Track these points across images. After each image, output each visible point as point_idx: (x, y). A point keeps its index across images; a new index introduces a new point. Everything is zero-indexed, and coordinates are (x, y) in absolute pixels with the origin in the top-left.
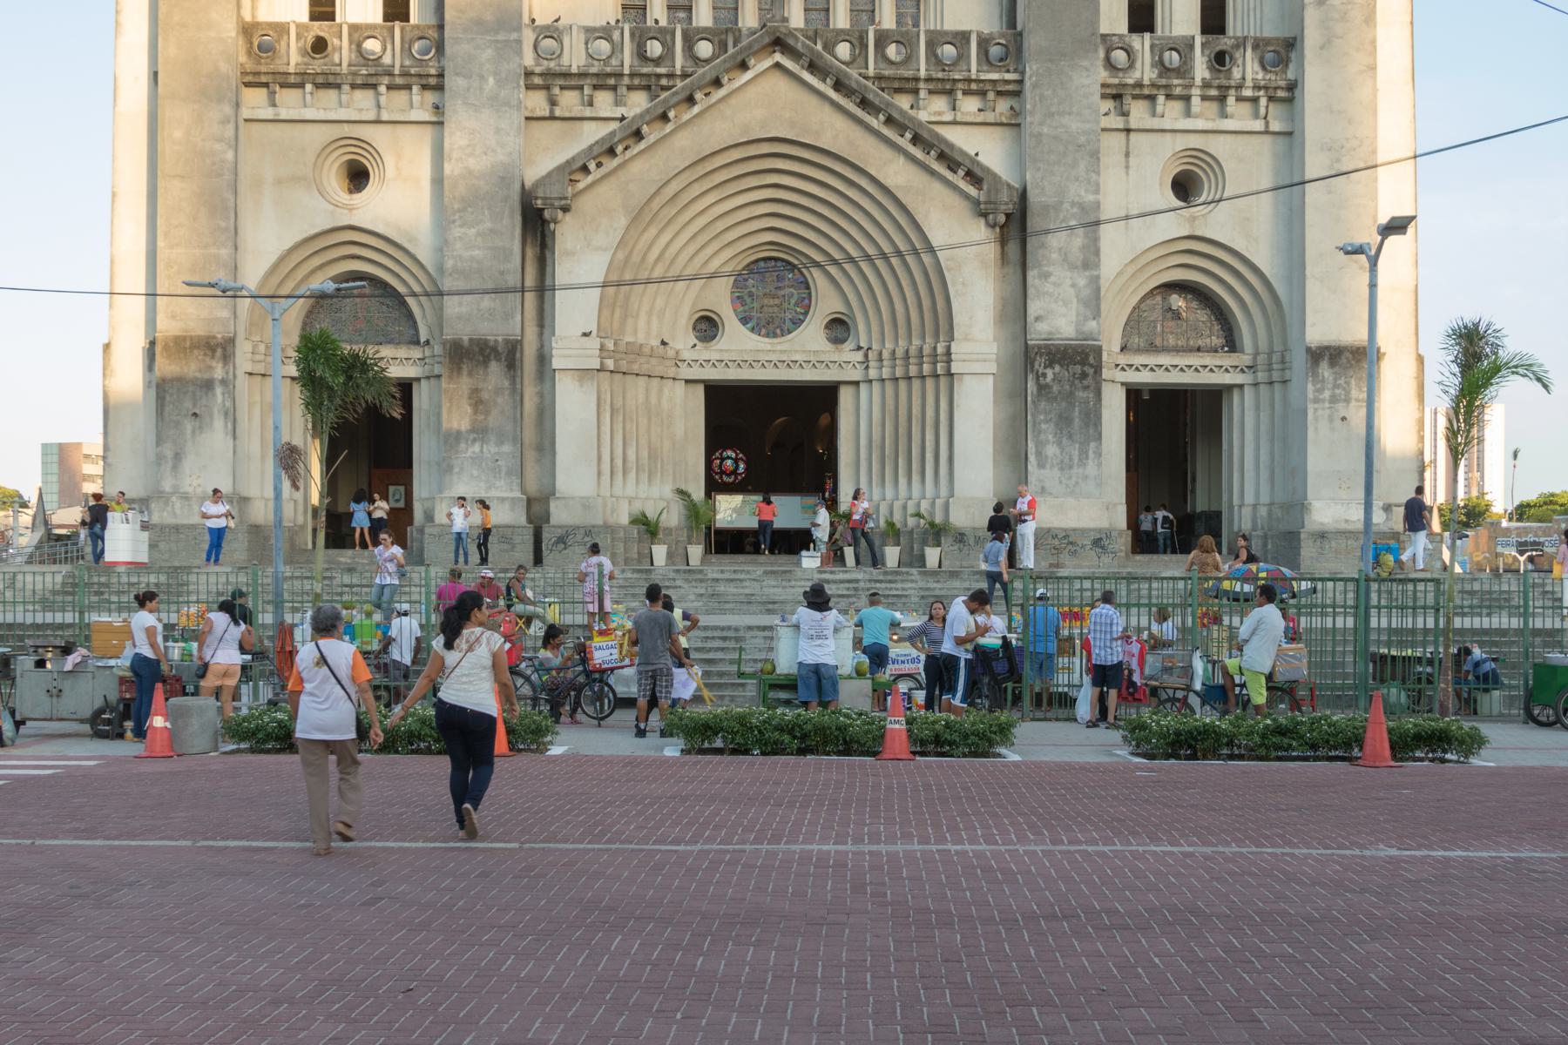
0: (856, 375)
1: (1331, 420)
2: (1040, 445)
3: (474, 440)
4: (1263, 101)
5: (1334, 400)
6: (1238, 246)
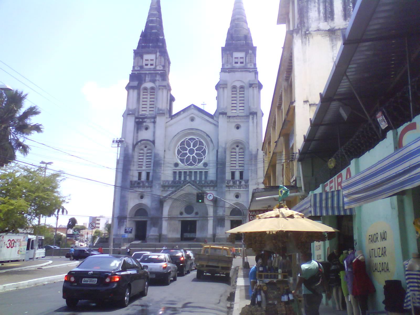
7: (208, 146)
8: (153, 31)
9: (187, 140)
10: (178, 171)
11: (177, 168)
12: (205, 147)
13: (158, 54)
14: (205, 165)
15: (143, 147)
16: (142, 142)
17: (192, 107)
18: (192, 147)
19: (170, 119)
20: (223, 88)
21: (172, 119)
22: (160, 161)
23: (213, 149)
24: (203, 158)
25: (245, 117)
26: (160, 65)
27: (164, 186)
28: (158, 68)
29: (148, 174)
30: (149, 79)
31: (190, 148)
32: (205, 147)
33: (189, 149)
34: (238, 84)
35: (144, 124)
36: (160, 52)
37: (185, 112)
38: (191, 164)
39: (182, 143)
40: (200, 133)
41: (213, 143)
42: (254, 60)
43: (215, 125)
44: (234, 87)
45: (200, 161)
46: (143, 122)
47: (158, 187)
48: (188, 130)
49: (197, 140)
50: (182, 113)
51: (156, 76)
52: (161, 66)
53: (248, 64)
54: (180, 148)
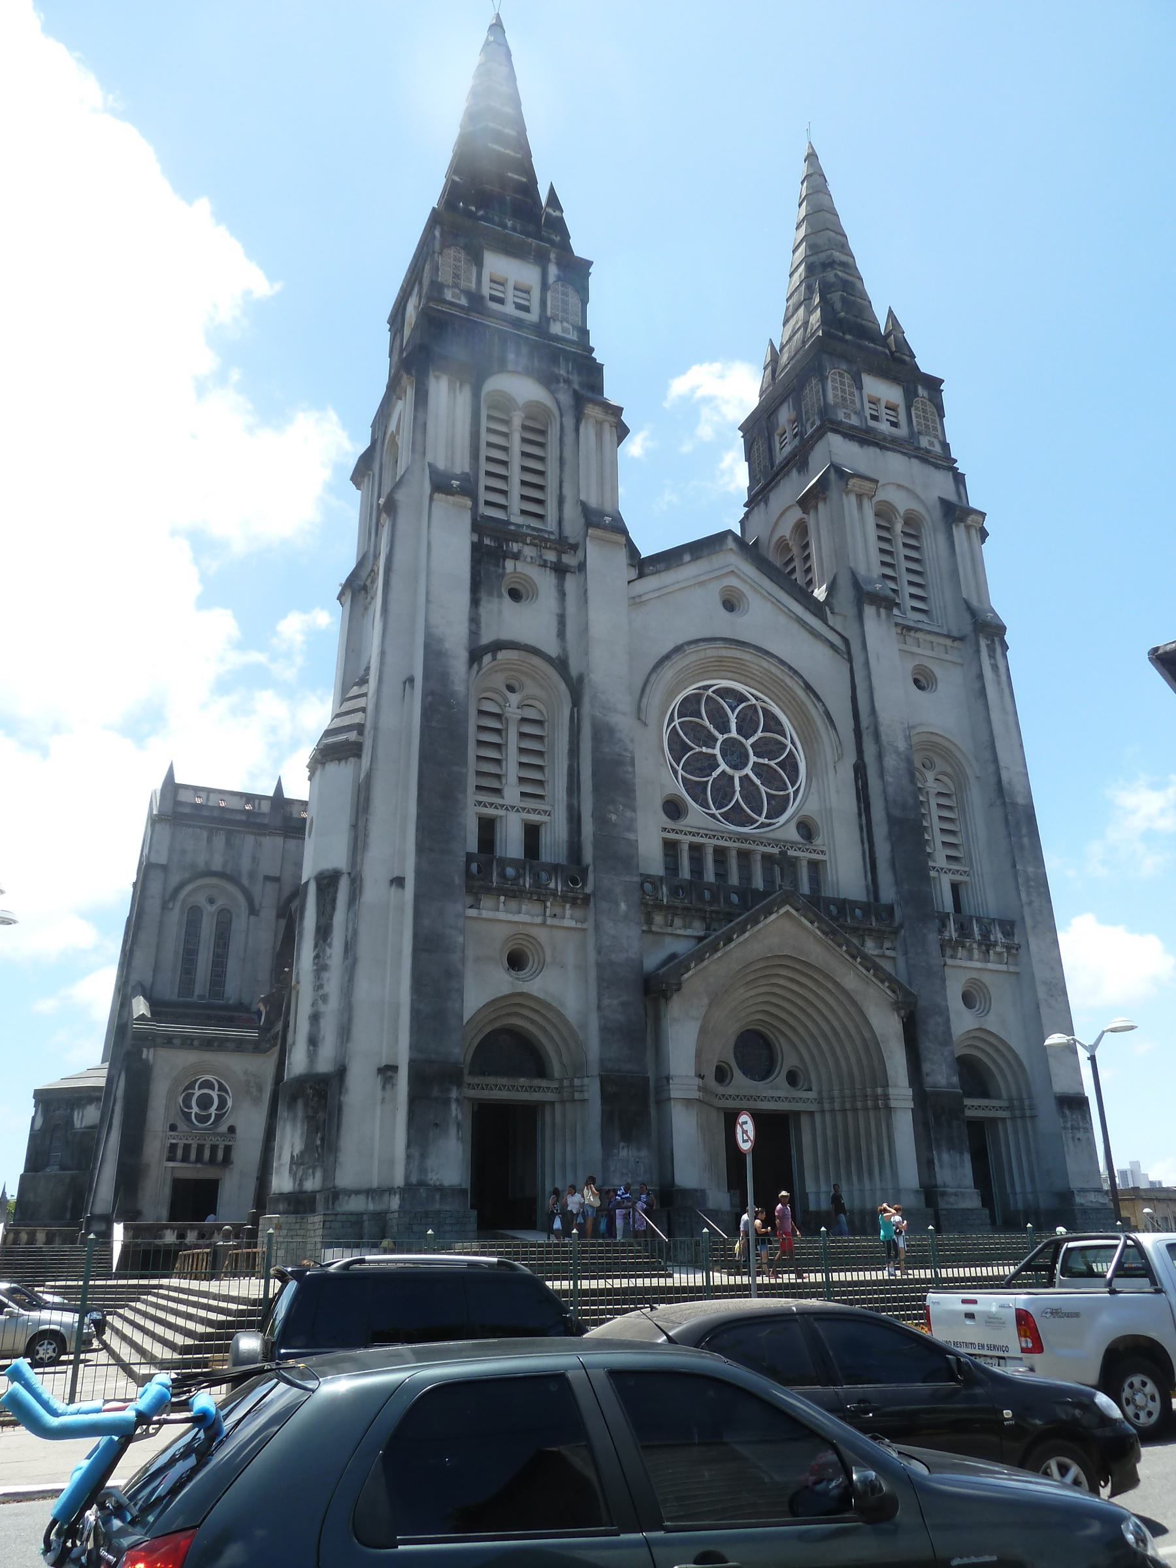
0: (813, 1107)
1: (1073, 1138)
2: (939, 1155)
3: (623, 1148)
4: (1005, 955)
5: (1073, 1128)
6: (1002, 1035)
7: (809, 739)
11: (681, 824)
12: (793, 743)
13: (553, 270)
14: (806, 829)
16: (502, 655)
17: (730, 543)
18: (734, 733)
21: (641, 575)
23: (841, 757)
24: (787, 792)
25: (948, 642)
27: (648, 908)
29: (532, 833)
31: (726, 736)
32: (793, 743)
33: (721, 738)
34: (902, 503)
35: (509, 565)
36: (559, 264)
37: (698, 558)
40: (773, 669)
41: (835, 729)
42: (939, 430)
43: (832, 646)
45: (779, 806)
47: (623, 906)
48: (720, 644)
49: (754, 701)
50: (687, 558)
53: (920, 433)
54: (678, 726)
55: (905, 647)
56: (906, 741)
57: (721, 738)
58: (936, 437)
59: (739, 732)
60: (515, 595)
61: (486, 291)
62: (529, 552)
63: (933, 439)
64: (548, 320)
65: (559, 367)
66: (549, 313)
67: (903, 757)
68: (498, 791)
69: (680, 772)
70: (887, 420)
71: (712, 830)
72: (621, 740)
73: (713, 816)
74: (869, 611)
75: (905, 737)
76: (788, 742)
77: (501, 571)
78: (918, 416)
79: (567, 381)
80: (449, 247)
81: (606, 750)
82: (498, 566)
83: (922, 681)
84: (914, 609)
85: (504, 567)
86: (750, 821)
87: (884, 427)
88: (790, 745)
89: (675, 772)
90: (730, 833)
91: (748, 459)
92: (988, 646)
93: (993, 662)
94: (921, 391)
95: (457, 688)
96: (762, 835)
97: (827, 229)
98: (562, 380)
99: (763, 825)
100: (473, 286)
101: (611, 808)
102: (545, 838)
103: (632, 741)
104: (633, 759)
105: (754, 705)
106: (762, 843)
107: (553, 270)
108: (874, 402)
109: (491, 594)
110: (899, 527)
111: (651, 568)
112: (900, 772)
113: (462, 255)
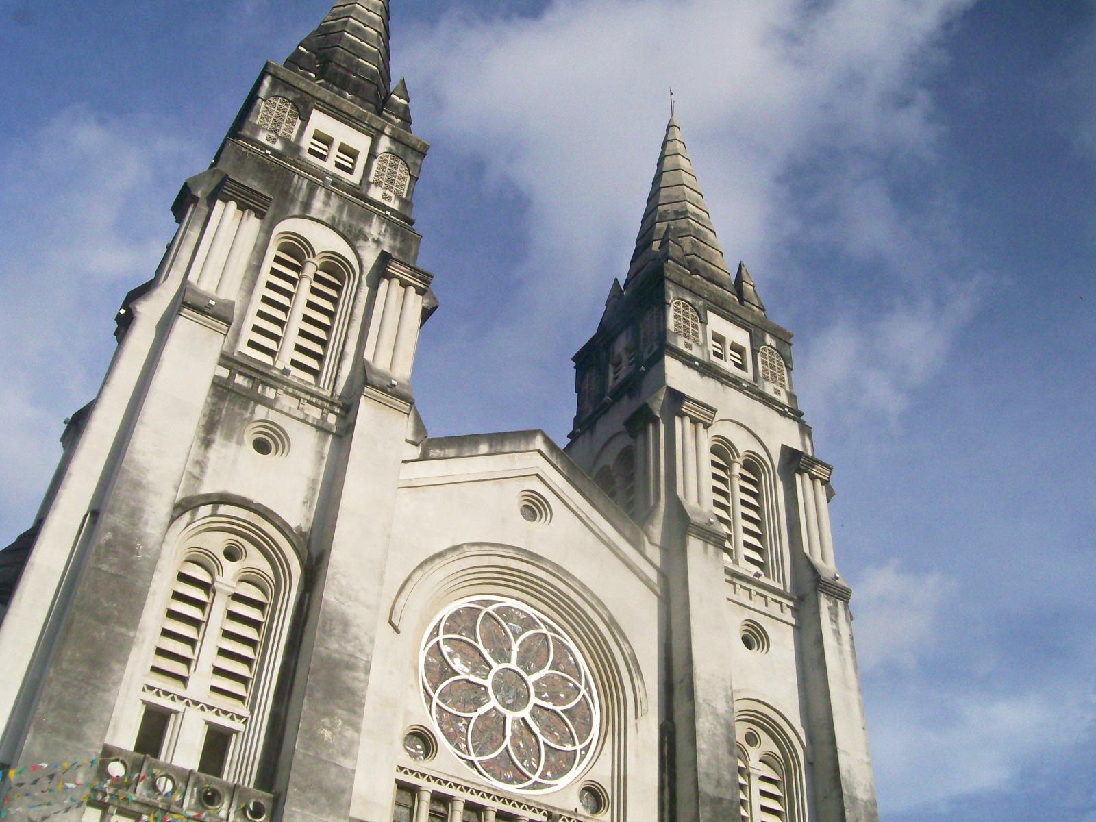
8: (360, 60)
9: (490, 609)
10: (429, 787)
11: (424, 766)
13: (385, 143)
15: (217, 542)
16: (224, 509)
17: (539, 443)
18: (513, 665)
19: (415, 452)
20: (694, 421)
21: (424, 457)
22: (351, 667)
26: (390, 189)
28: (376, 193)
29: (217, 742)
30: (331, 211)
33: (496, 667)
34: (743, 444)
35: (261, 412)
38: (505, 768)
39: (463, 620)
41: (642, 678)
44: (722, 450)
45: (560, 764)
46: (249, 398)
49: (544, 630)
50: (484, 448)
51: (367, 219)
52: (393, 196)
55: (734, 597)
56: (728, 703)
57: (496, 667)
58: (783, 386)
59: (520, 663)
60: (262, 446)
61: (307, 142)
62: (287, 402)
63: (779, 388)
64: (369, 184)
65: (370, 225)
66: (372, 178)
67: (722, 721)
68: (184, 680)
69: (436, 699)
70: (731, 360)
71: (465, 781)
72: (356, 638)
73: (471, 764)
74: (695, 545)
75: (727, 696)
76: (582, 687)
77: (248, 415)
78: (764, 363)
79: (377, 242)
80: (276, 97)
81: (334, 645)
82: (246, 409)
83: (753, 638)
84: (748, 559)
85: (253, 412)
86: (521, 777)
87: (728, 366)
88: (583, 691)
89: (429, 699)
90: (489, 788)
91: (578, 390)
92: (829, 608)
93: (834, 627)
94: (769, 340)
95: (149, 530)
96: (531, 798)
97: (683, 184)
98: (370, 239)
99: (537, 785)
100: (293, 136)
101: (326, 720)
102: (234, 751)
103: (372, 641)
104: (369, 663)
105: (545, 635)
106: (530, 807)
107: (385, 143)
108: (719, 339)
109: (228, 437)
110: (737, 469)
111: (438, 451)
112: (717, 739)
113: (289, 107)
